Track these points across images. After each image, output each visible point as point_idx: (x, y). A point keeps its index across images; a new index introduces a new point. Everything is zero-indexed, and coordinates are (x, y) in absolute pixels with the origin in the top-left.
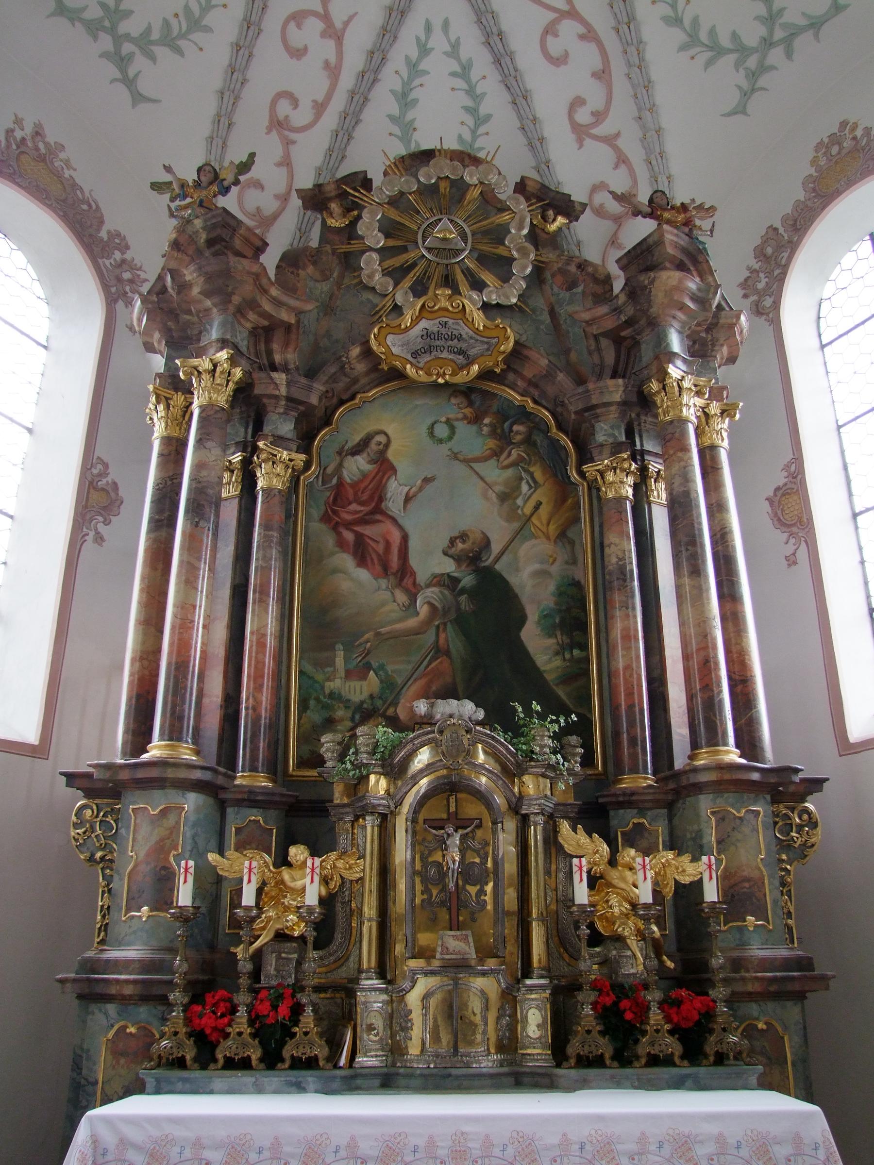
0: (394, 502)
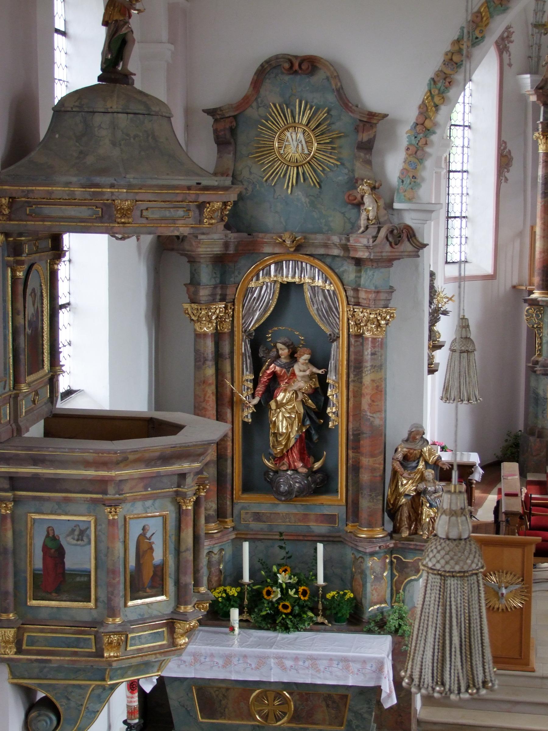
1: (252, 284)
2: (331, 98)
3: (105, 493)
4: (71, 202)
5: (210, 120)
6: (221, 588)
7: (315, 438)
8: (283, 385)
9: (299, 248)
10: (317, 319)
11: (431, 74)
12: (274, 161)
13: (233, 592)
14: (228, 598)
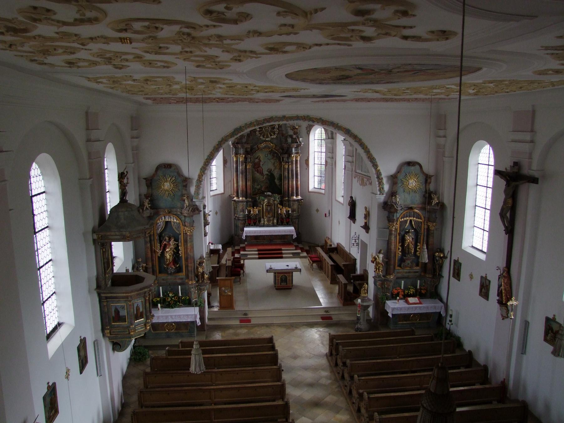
0: (261, 165)
1: (158, 222)
2: (176, 174)
3: (128, 298)
4: (116, 235)
5: (145, 180)
6: (155, 299)
7: (177, 259)
8: (168, 247)
9: (169, 213)
10: (175, 230)
11: (200, 167)
12: (162, 190)
13: (158, 299)
14: (157, 301)
